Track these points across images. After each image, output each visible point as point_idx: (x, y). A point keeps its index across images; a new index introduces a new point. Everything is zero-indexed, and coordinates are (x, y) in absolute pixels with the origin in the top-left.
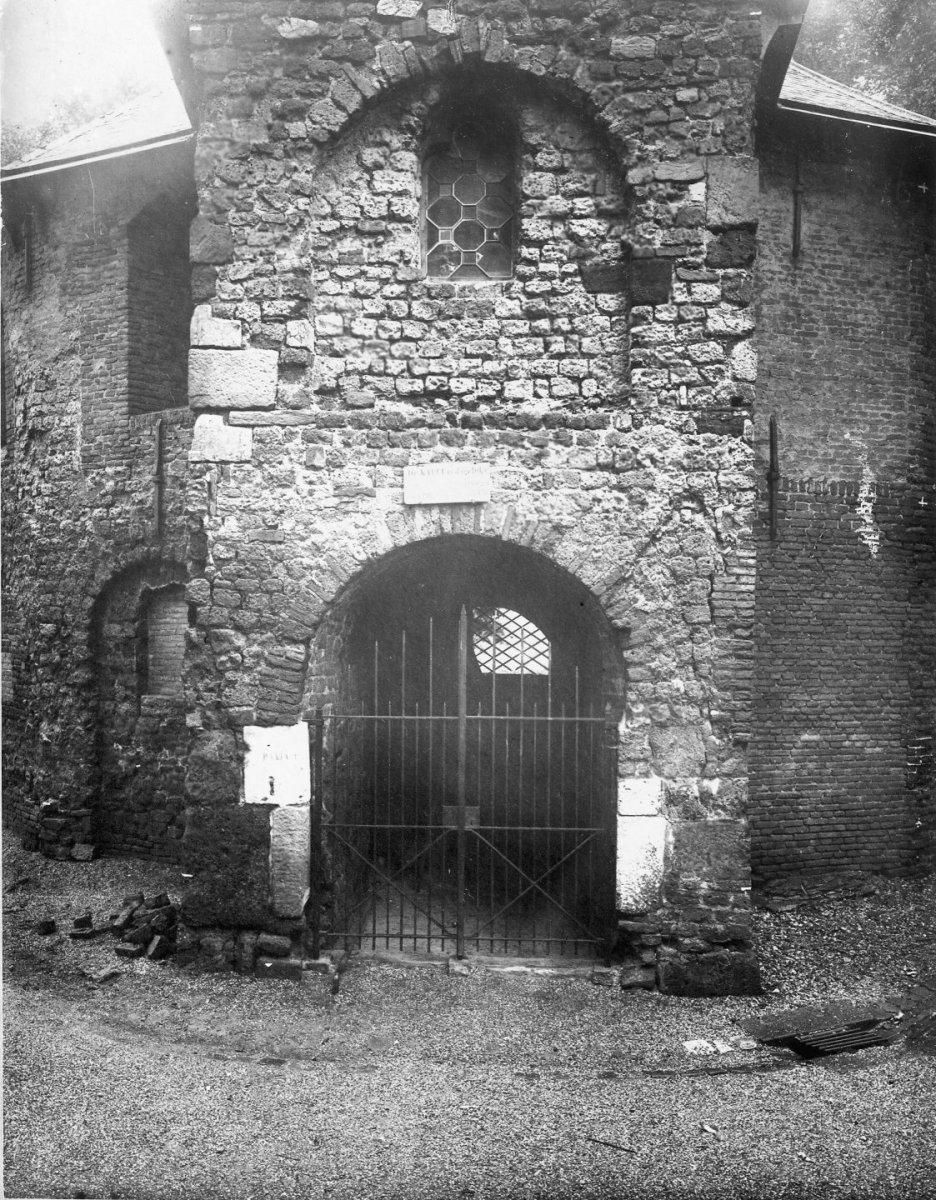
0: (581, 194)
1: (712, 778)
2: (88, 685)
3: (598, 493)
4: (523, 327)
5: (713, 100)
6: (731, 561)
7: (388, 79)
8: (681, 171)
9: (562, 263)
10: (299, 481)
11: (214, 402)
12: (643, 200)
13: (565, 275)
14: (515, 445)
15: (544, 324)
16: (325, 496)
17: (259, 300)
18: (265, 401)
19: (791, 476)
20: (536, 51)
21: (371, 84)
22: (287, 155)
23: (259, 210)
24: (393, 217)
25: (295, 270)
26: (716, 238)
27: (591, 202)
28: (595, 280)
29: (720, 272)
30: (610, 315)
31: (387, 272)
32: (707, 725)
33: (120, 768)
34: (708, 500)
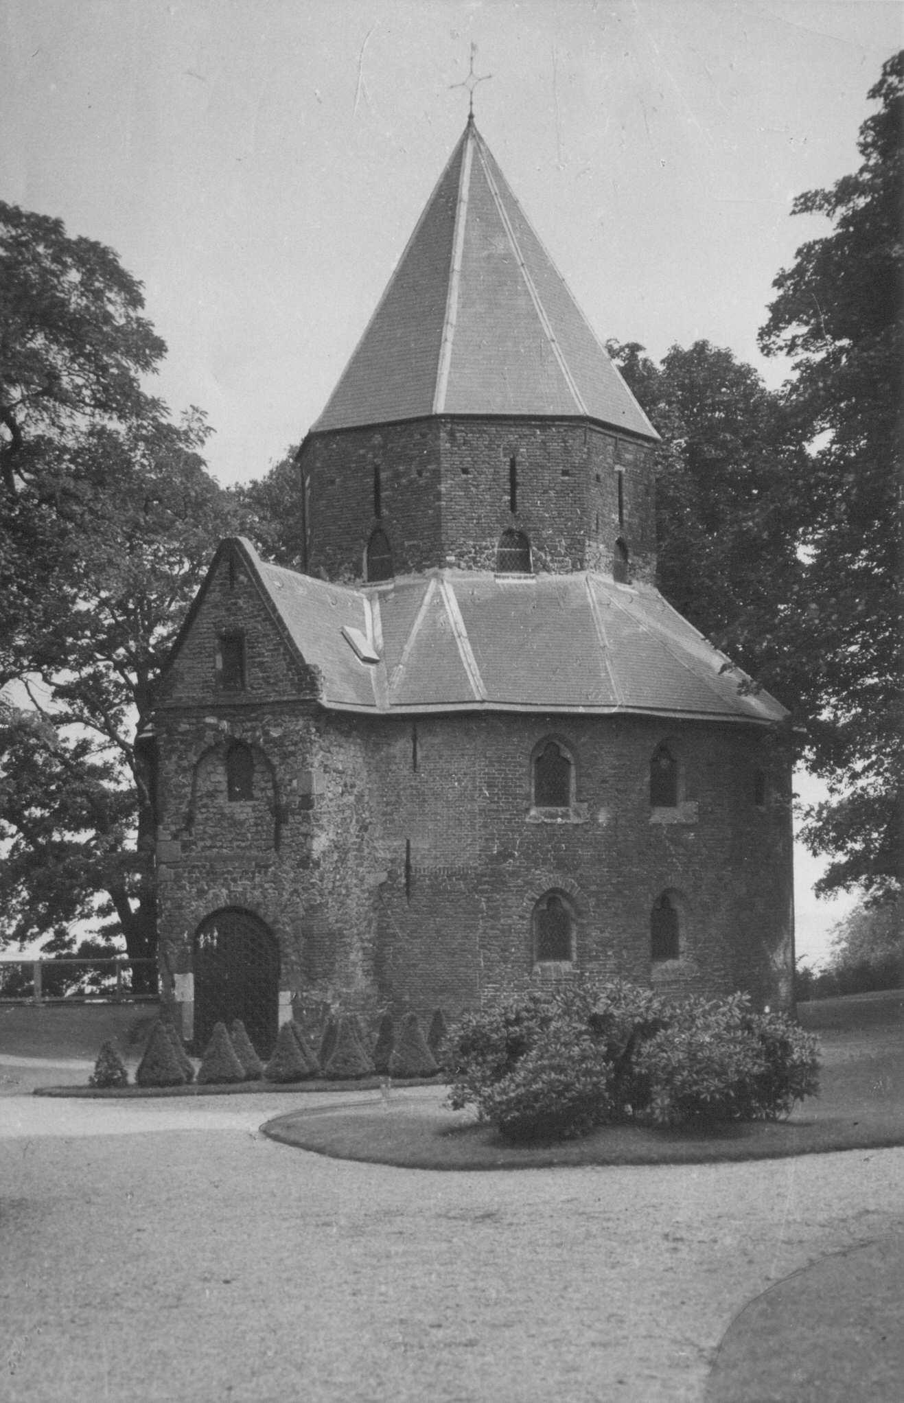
4: (254, 829)
15: (260, 828)
21: (204, 746)
24: (217, 791)
31: (215, 810)
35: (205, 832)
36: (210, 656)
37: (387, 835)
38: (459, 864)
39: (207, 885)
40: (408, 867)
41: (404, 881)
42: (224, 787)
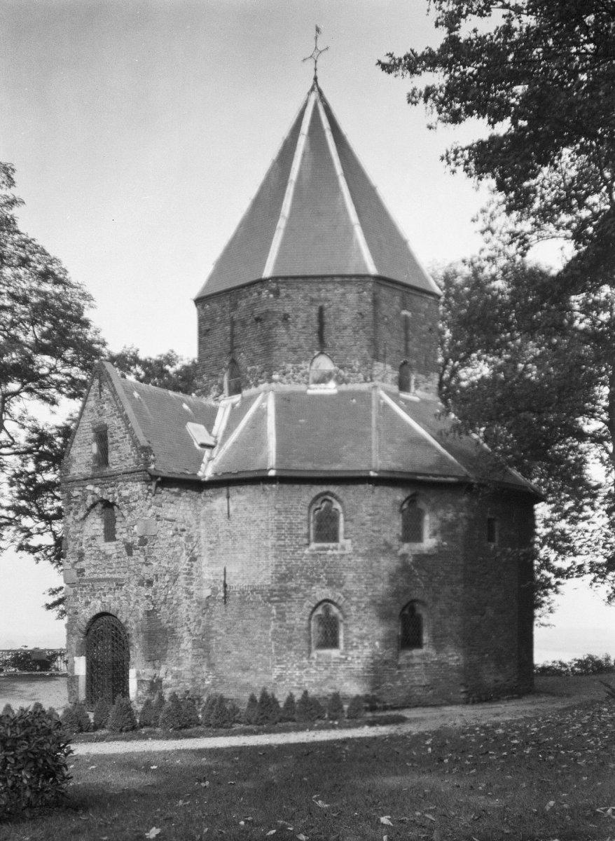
19: (231, 585)
21: (88, 506)
35: (91, 563)
36: (90, 444)
37: (211, 563)
40: (225, 586)
41: (222, 595)
42: (101, 532)
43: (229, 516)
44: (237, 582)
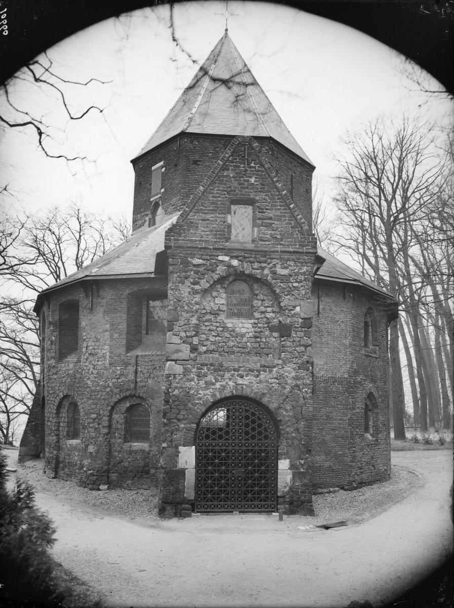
0: (269, 307)
1: (302, 459)
2: (107, 434)
3: (274, 385)
5: (302, 286)
6: (307, 403)
7: (221, 276)
8: (293, 303)
9: (263, 324)
10: (196, 380)
11: (172, 359)
12: (285, 310)
13: (264, 328)
14: (252, 372)
15: (259, 339)
16: (202, 383)
17: (185, 332)
18: (186, 359)
19: (317, 375)
20: (258, 271)
21: (216, 277)
22: (194, 294)
23: (186, 308)
25: (195, 324)
26: (302, 321)
27: (271, 309)
28: (272, 329)
29: (304, 329)
30: (276, 338)
32: (301, 445)
33: (117, 460)
34: (301, 387)
38: (339, 375)
39: (215, 379)
43: (319, 313)
44: (322, 373)
